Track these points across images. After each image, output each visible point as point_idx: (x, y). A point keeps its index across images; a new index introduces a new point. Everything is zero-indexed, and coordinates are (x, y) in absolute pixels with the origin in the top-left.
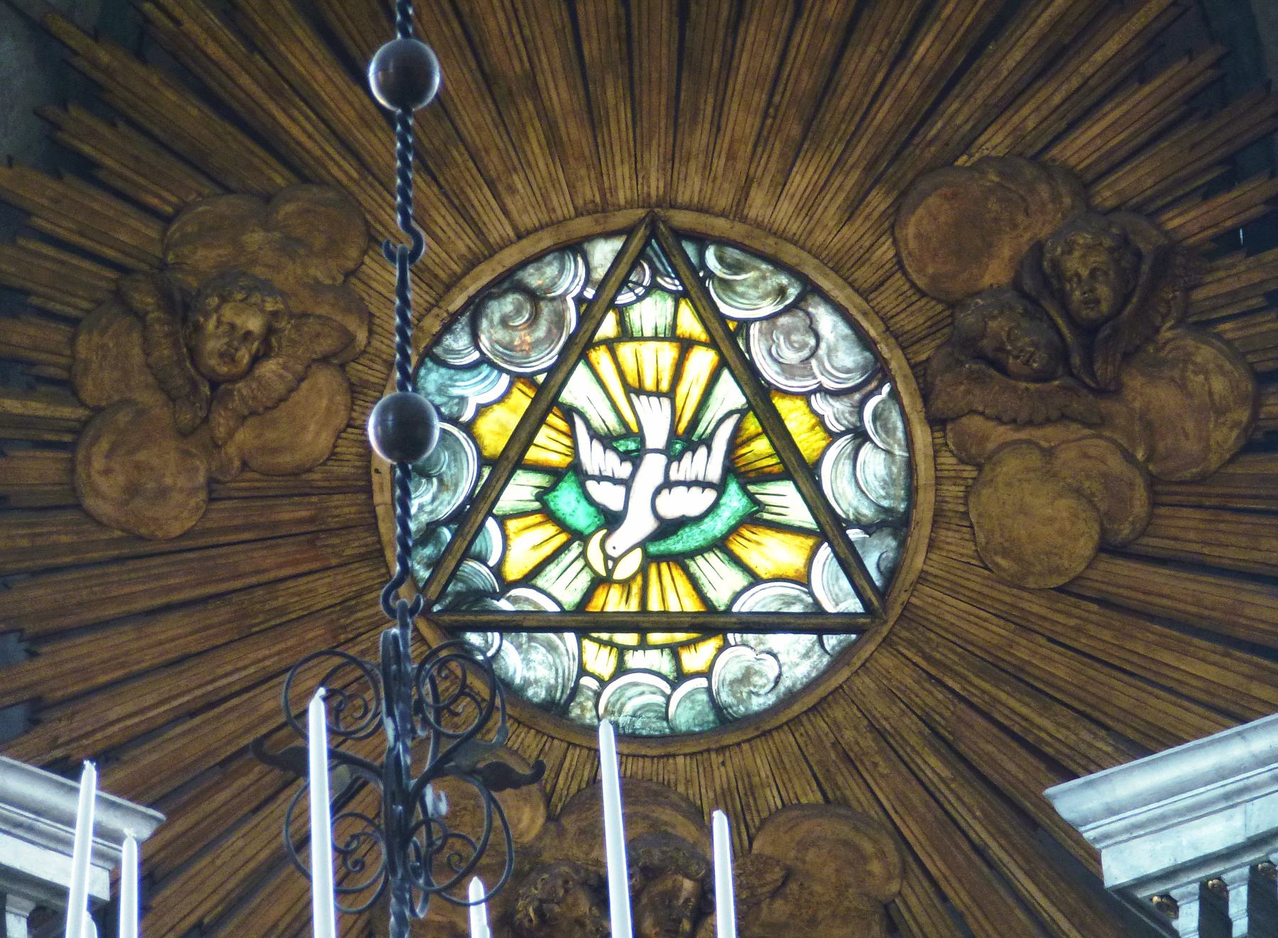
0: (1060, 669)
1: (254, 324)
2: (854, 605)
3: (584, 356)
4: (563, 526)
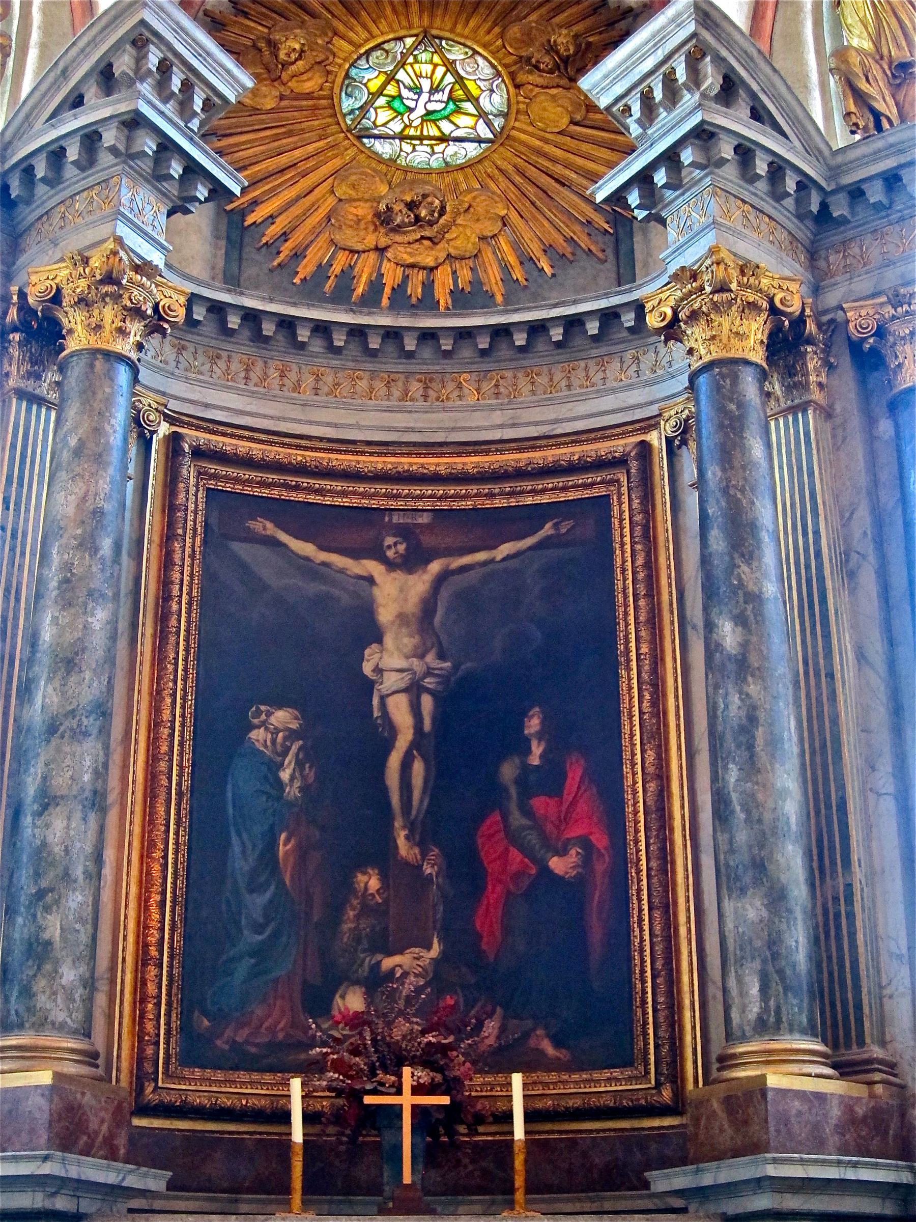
0: (559, 153)
1: (297, 46)
2: (491, 136)
3: (403, 66)
4: (396, 111)
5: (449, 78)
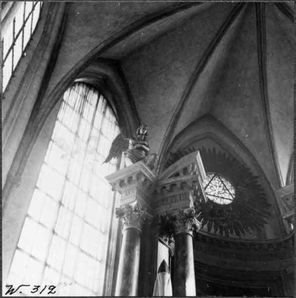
5: (222, 185)
